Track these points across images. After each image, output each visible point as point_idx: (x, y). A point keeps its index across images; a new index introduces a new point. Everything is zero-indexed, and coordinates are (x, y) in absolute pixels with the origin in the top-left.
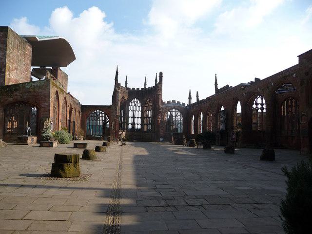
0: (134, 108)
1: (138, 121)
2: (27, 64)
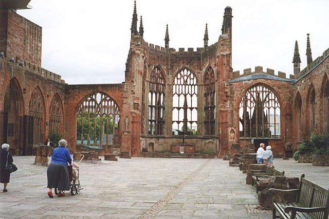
0: (182, 89)
1: (193, 116)
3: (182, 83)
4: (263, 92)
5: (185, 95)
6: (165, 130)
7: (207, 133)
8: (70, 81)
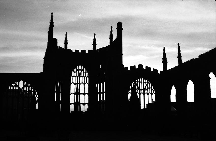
1: (84, 99)
3: (77, 75)
4: (144, 82)
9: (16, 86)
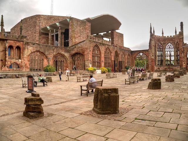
1: (173, 58)
2: (88, 33)
5: (170, 52)
6: (163, 64)
7: (177, 64)
8: (132, 50)
9: (139, 55)
